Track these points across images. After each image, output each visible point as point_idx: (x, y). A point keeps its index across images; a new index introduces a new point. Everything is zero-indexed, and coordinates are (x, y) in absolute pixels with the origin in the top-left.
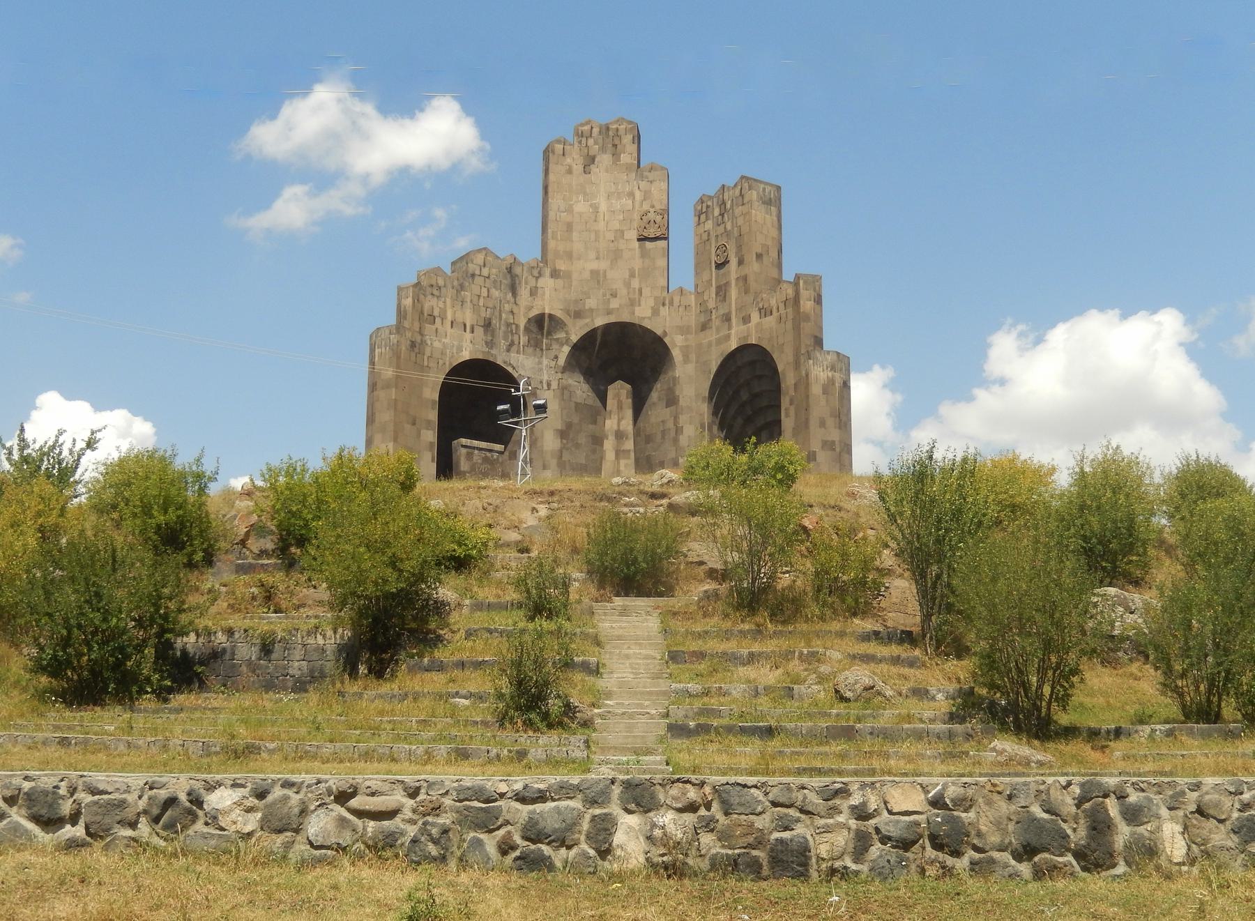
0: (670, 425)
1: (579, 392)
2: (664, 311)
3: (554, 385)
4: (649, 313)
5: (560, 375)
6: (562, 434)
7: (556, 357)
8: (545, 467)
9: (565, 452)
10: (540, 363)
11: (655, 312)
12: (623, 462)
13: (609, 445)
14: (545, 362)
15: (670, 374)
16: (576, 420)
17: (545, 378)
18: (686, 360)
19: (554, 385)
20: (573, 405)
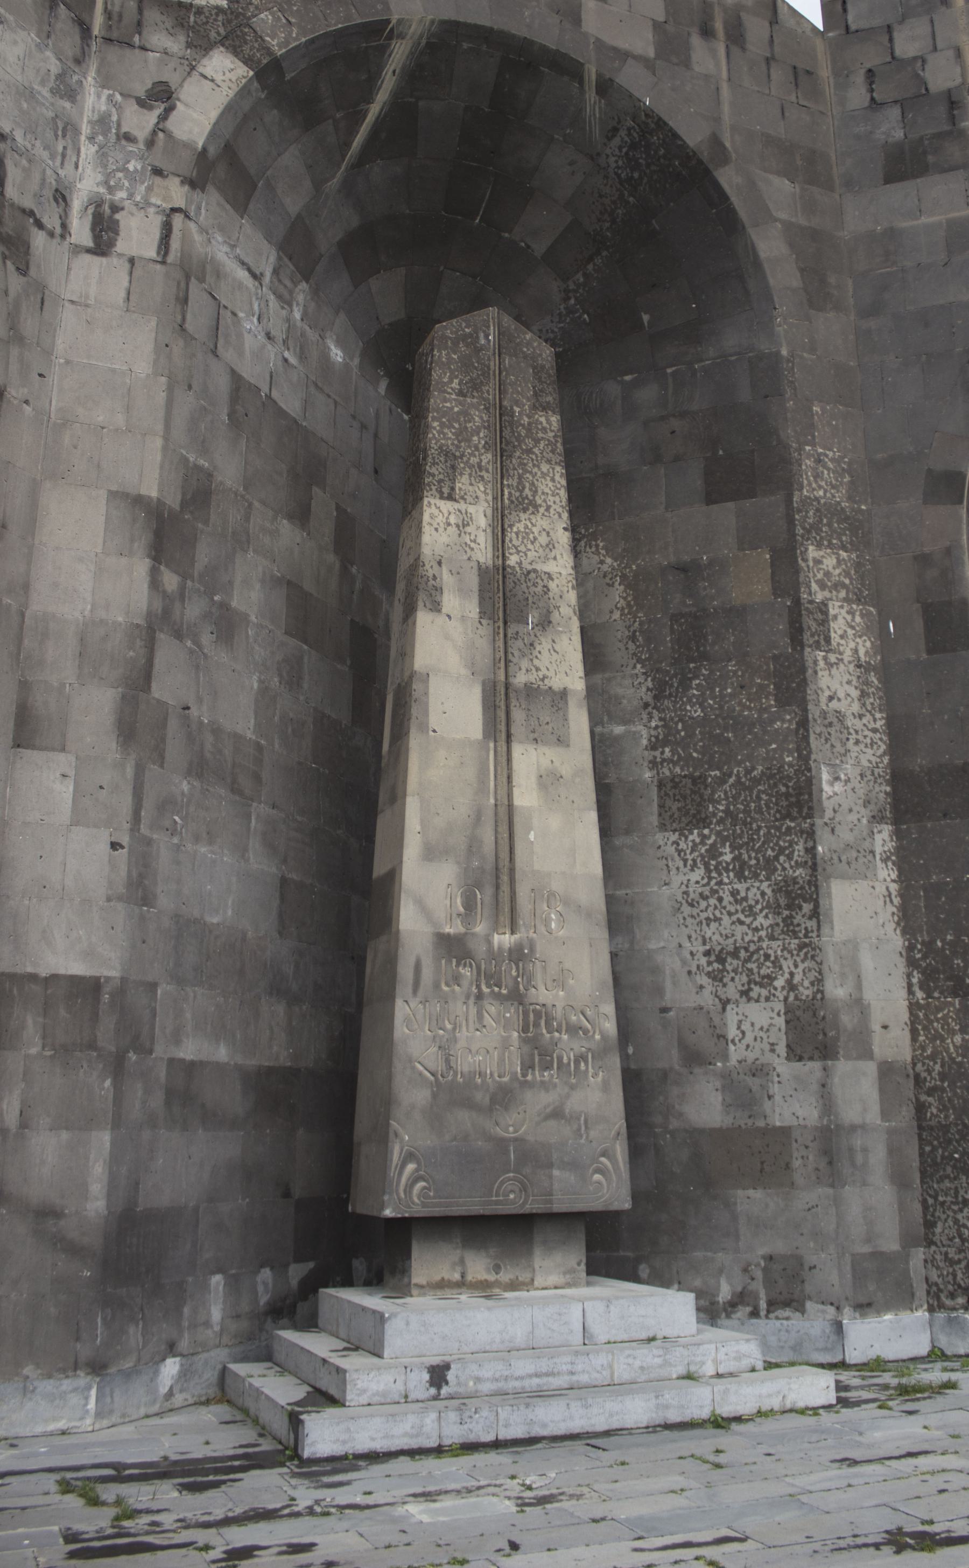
0: (750, 583)
1: (250, 324)
2: (709, 58)
3: (138, 235)
4: (642, 43)
5: (177, 193)
6: (166, 531)
7: (162, 96)
8: (27, 731)
9: (168, 653)
10: (68, 91)
11: (671, 48)
12: (528, 760)
13: (444, 648)
14: (93, 100)
15: (731, 340)
16: (228, 469)
17: (87, 184)
18: (817, 295)
19: (138, 235)
20: (222, 384)
